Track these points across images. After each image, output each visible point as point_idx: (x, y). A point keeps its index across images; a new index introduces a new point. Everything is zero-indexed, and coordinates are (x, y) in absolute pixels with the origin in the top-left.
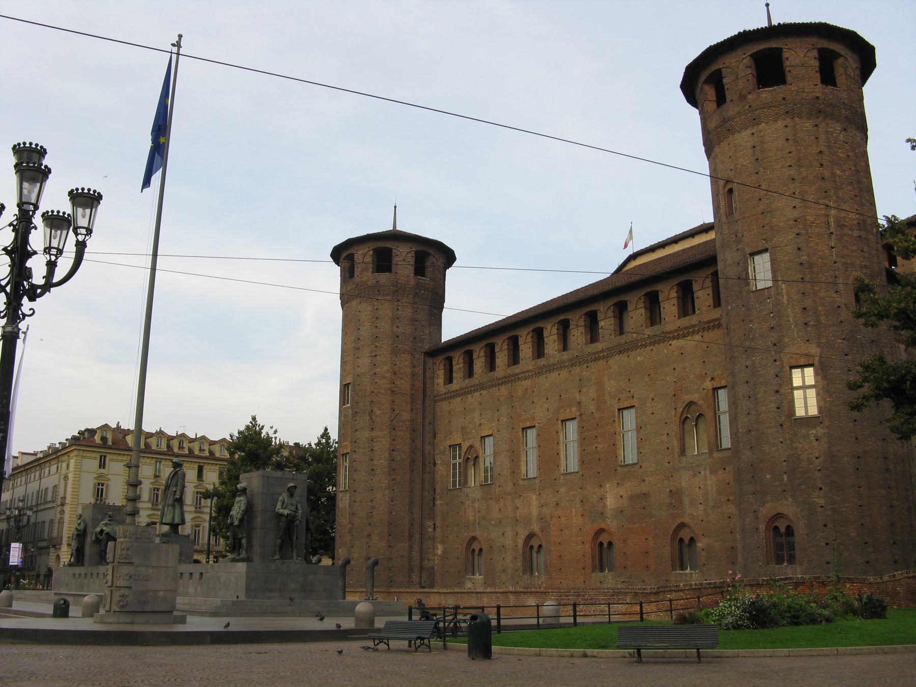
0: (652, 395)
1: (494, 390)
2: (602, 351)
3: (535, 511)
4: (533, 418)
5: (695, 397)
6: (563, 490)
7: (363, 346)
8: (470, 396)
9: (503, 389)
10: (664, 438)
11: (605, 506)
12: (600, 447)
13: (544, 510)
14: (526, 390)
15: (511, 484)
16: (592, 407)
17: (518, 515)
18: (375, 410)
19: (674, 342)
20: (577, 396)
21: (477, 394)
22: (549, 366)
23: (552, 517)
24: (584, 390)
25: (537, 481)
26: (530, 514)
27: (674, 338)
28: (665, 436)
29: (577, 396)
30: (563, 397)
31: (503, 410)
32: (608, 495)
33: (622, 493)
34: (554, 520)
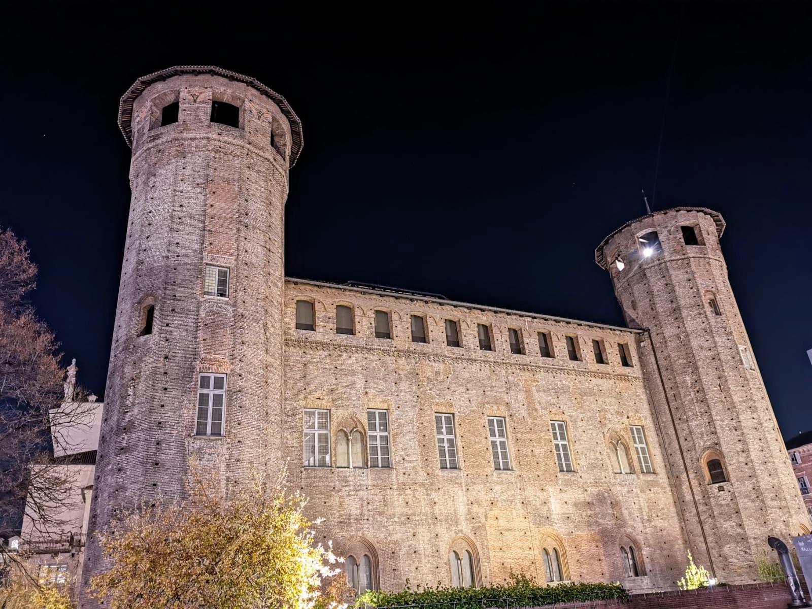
0: (581, 416)
1: (389, 360)
3: (462, 510)
4: (451, 406)
6: (497, 488)
7: (254, 228)
8: (345, 356)
9: (402, 361)
10: (598, 455)
11: (549, 510)
12: (537, 452)
13: (475, 508)
14: (438, 373)
15: (422, 476)
16: (523, 412)
17: (437, 511)
18: (269, 325)
19: (593, 379)
20: (504, 396)
21: (360, 355)
23: (486, 518)
24: (512, 393)
25: (462, 474)
26: (455, 511)
28: (598, 453)
29: (506, 398)
30: (488, 393)
31: (406, 386)
32: (552, 500)
33: (566, 500)
34: (491, 521)
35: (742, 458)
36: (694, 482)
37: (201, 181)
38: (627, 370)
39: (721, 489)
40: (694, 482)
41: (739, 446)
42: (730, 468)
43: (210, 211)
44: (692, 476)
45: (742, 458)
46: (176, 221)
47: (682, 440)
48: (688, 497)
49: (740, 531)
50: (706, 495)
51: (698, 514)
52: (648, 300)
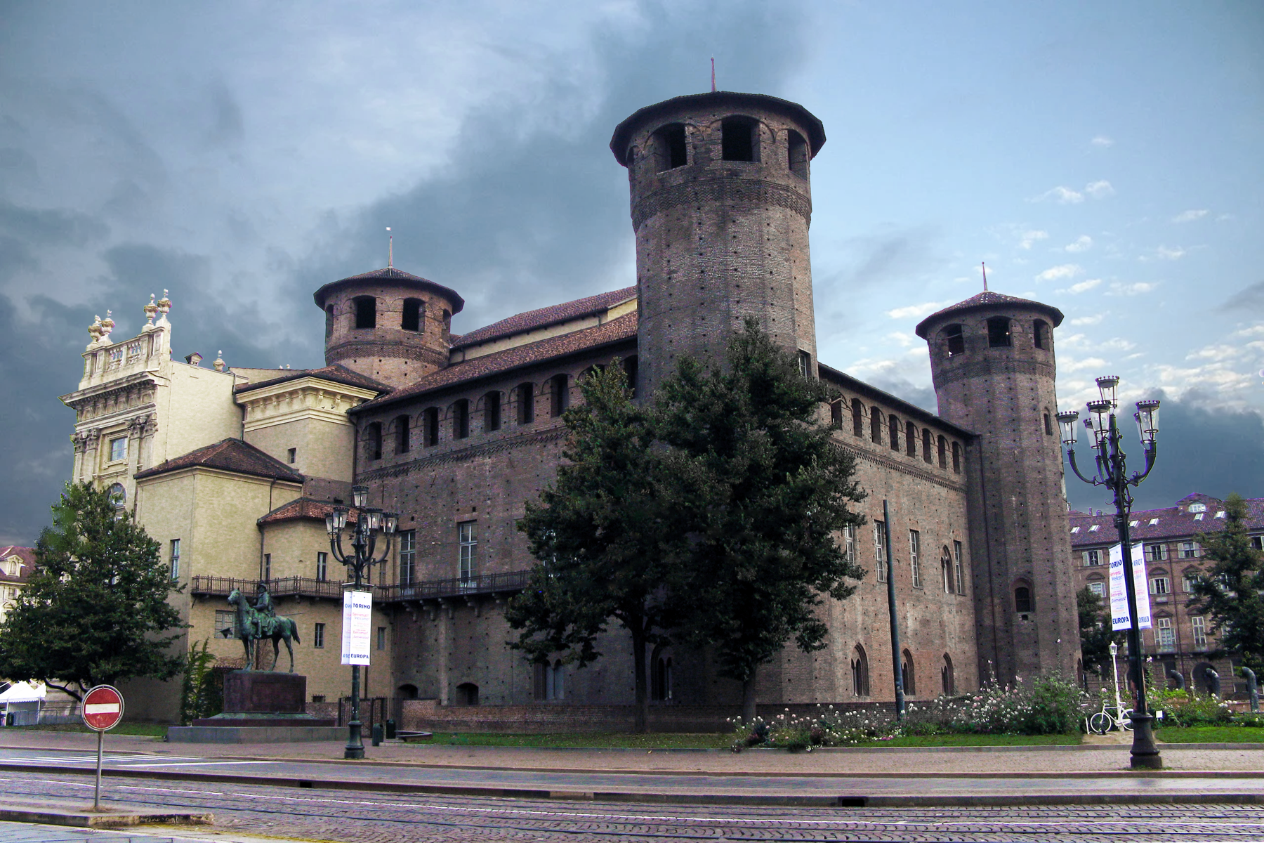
2: (900, 463)
5: (946, 542)
22: (866, 451)
27: (937, 482)
35: (1049, 590)
36: (998, 609)
37: (783, 245)
38: (955, 478)
39: (1025, 617)
40: (998, 609)
41: (1047, 578)
42: (1037, 598)
43: (795, 285)
44: (996, 601)
45: (1049, 590)
46: (769, 292)
47: (994, 563)
48: (988, 622)
49: (1035, 660)
50: (1008, 622)
51: (995, 640)
52: (986, 400)
